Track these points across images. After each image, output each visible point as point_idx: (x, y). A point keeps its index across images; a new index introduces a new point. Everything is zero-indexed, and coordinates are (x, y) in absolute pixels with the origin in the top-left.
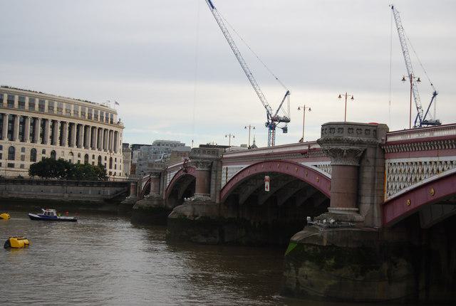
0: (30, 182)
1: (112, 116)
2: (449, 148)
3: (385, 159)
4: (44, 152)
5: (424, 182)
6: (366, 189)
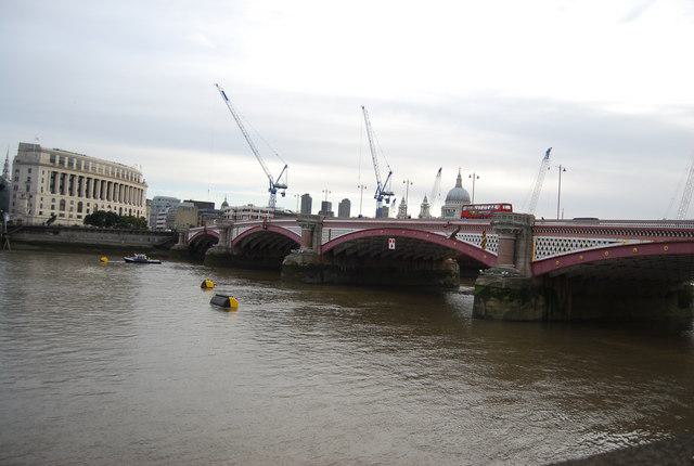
0: (86, 230)
4: (88, 205)
6: (521, 254)
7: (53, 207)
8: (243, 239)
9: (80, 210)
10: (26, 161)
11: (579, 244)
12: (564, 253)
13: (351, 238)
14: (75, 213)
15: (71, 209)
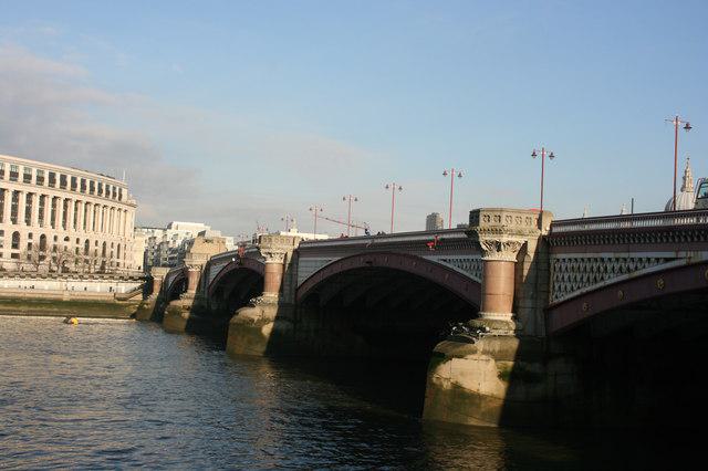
1: (120, 190)
2: (680, 241)
3: (549, 253)
4: (30, 236)
5: (608, 282)
11: (617, 266)
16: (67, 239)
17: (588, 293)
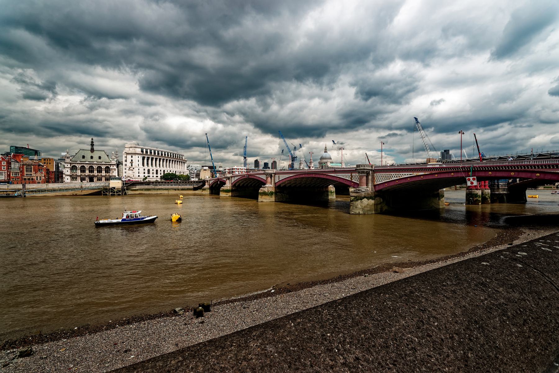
6: (370, 182)
7: (144, 173)
8: (237, 182)
9: (157, 173)
10: (130, 152)
11: (396, 176)
12: (389, 180)
13: (288, 179)
14: (155, 175)
15: (153, 173)
16: (170, 171)
17: (387, 182)
